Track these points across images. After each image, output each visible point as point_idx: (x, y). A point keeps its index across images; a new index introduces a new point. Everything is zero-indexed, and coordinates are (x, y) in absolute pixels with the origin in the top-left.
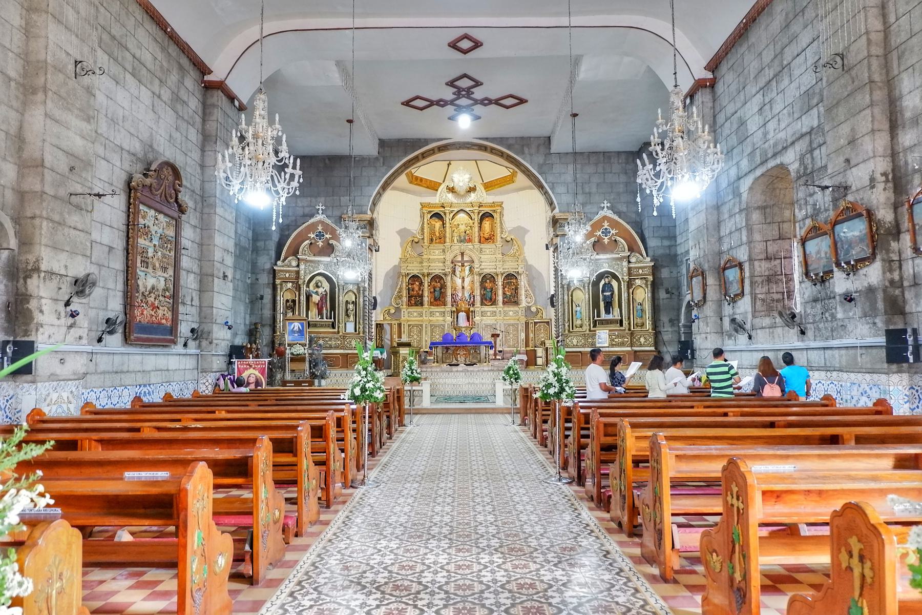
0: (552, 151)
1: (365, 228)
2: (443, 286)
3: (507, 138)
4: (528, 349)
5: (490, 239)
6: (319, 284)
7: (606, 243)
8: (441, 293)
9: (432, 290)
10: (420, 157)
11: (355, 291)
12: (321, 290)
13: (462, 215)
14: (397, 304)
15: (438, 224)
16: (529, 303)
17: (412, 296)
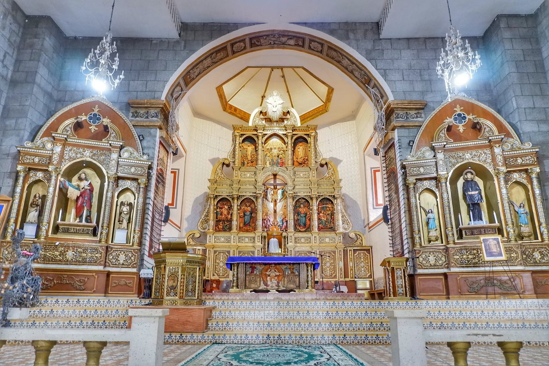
0: (381, 37)
1: (157, 116)
2: (254, 211)
3: (329, 23)
4: (347, 279)
5: (304, 163)
6: (83, 176)
7: (461, 130)
8: (251, 217)
9: (242, 214)
10: (229, 48)
11: (133, 189)
12: (84, 184)
13: (275, 140)
14: (204, 229)
15: (250, 148)
16: (345, 229)
17: (220, 221)
